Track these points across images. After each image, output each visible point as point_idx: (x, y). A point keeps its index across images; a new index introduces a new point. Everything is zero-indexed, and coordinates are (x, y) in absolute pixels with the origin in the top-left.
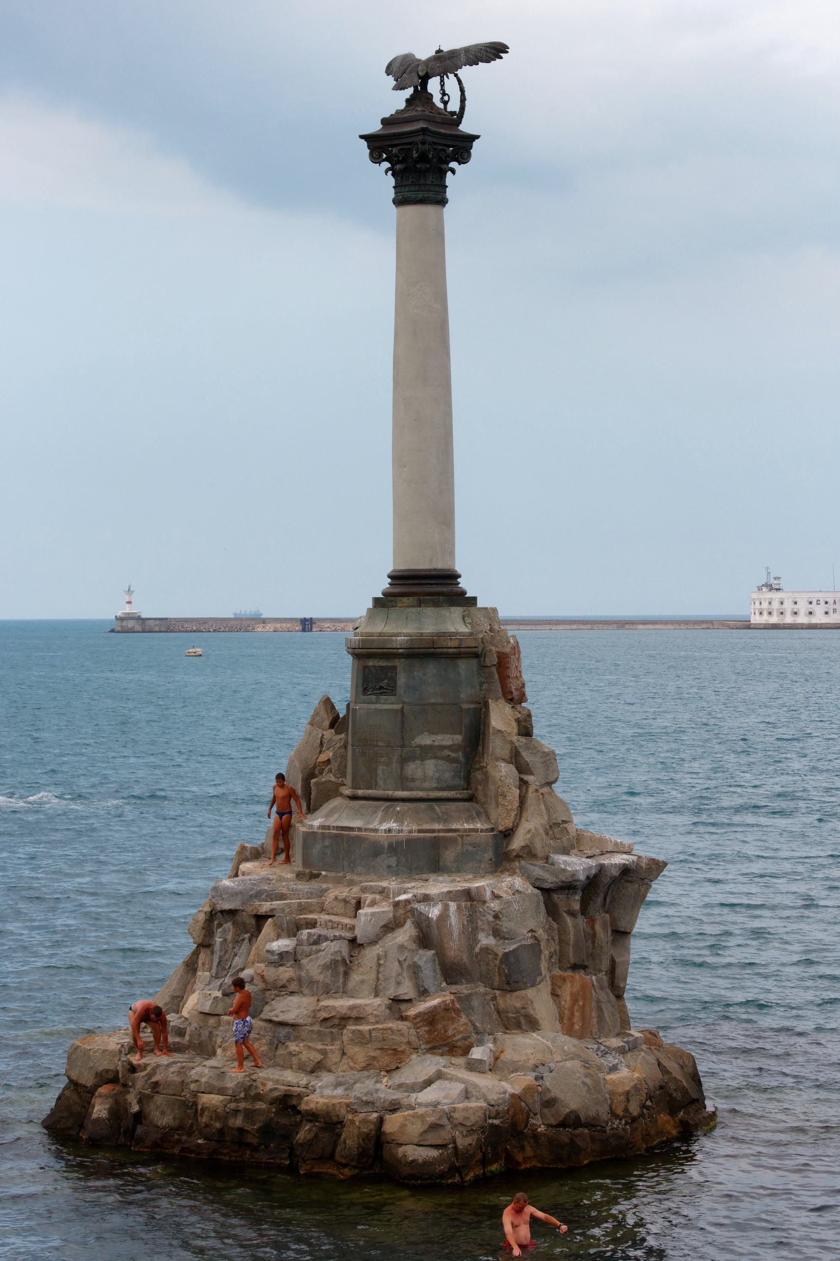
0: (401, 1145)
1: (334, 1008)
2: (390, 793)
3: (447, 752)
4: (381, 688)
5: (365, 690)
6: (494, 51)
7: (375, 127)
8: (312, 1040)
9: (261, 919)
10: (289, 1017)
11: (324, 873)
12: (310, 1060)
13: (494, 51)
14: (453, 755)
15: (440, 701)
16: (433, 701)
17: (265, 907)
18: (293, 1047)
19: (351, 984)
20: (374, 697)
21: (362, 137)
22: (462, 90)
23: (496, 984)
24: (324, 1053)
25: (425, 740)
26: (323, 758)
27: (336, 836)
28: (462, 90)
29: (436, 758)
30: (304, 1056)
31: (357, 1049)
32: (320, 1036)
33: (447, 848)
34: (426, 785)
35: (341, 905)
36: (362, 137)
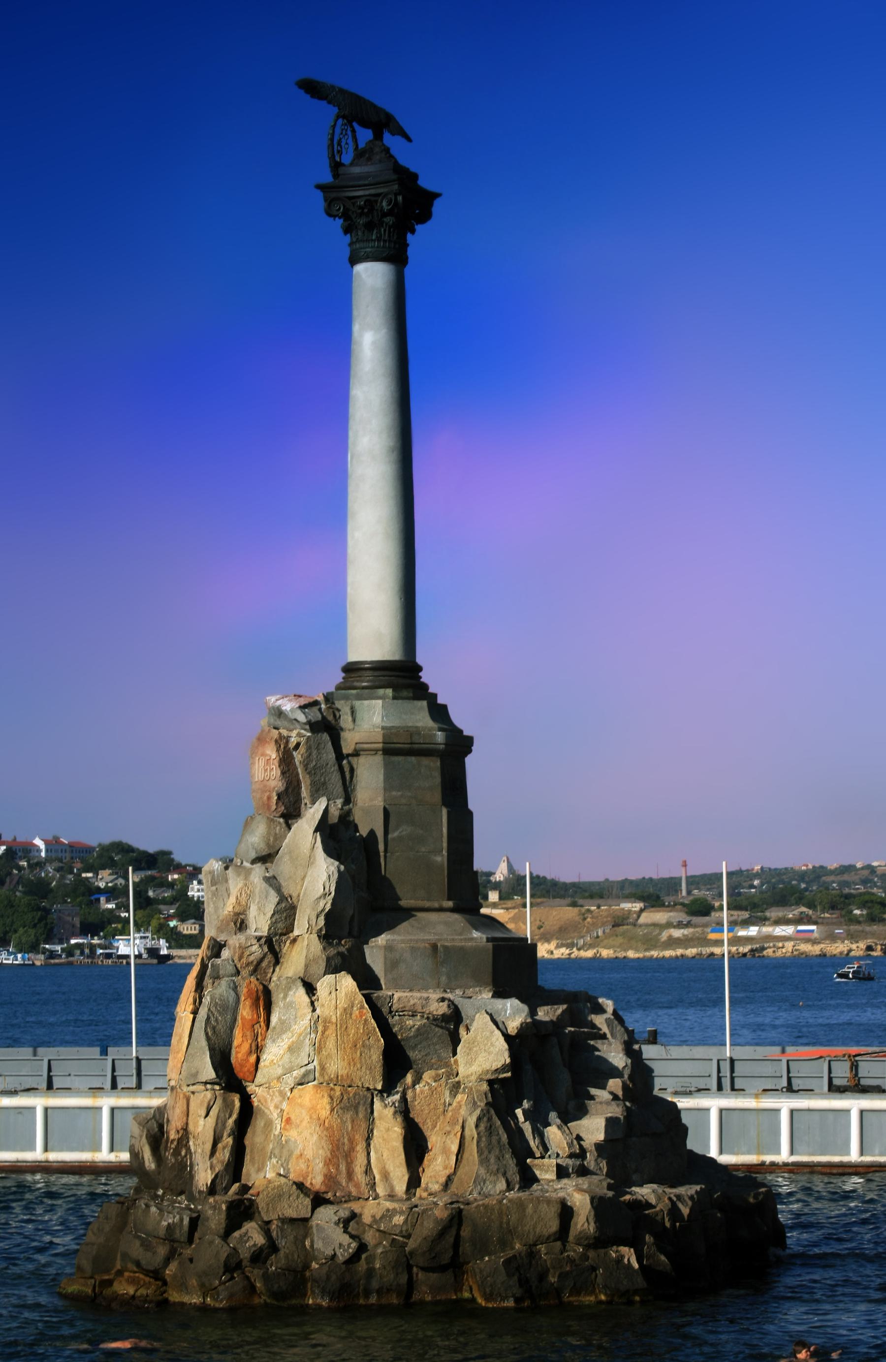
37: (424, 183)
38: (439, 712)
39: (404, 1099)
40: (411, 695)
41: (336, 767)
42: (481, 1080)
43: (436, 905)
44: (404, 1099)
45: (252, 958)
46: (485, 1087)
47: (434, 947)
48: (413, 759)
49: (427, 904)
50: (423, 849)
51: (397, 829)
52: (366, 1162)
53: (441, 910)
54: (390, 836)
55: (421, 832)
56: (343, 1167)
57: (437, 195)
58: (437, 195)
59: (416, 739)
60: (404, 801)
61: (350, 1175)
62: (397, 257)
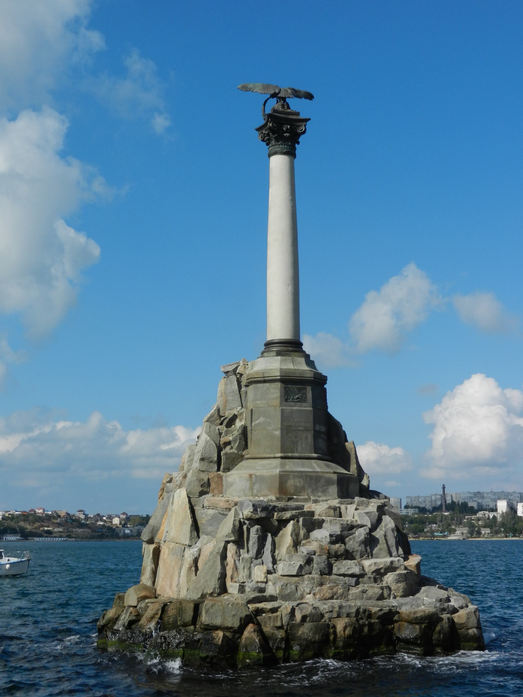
0: (469, 629)
1: (381, 563)
2: (310, 455)
5: (286, 400)
6: (309, 96)
8: (371, 583)
9: (283, 523)
10: (356, 570)
11: (295, 497)
12: (376, 593)
13: (309, 96)
17: (288, 515)
18: (360, 587)
19: (374, 552)
20: (293, 403)
24: (382, 588)
25: (318, 427)
26: (223, 440)
30: (370, 592)
31: (399, 585)
32: (375, 581)
35: (332, 511)
37: (302, 116)
38: (310, 363)
39: (200, 550)
40: (275, 354)
41: (238, 392)
42: (222, 541)
43: (272, 456)
44: (200, 550)
45: (177, 483)
46: (223, 544)
47: (251, 476)
48: (267, 385)
49: (268, 456)
50: (270, 428)
51: (258, 419)
52: (177, 581)
53: (275, 458)
54: (253, 424)
55: (269, 420)
56: (168, 583)
57: (309, 119)
58: (309, 119)
59: (266, 375)
60: (262, 406)
61: (171, 586)
62: (291, 153)
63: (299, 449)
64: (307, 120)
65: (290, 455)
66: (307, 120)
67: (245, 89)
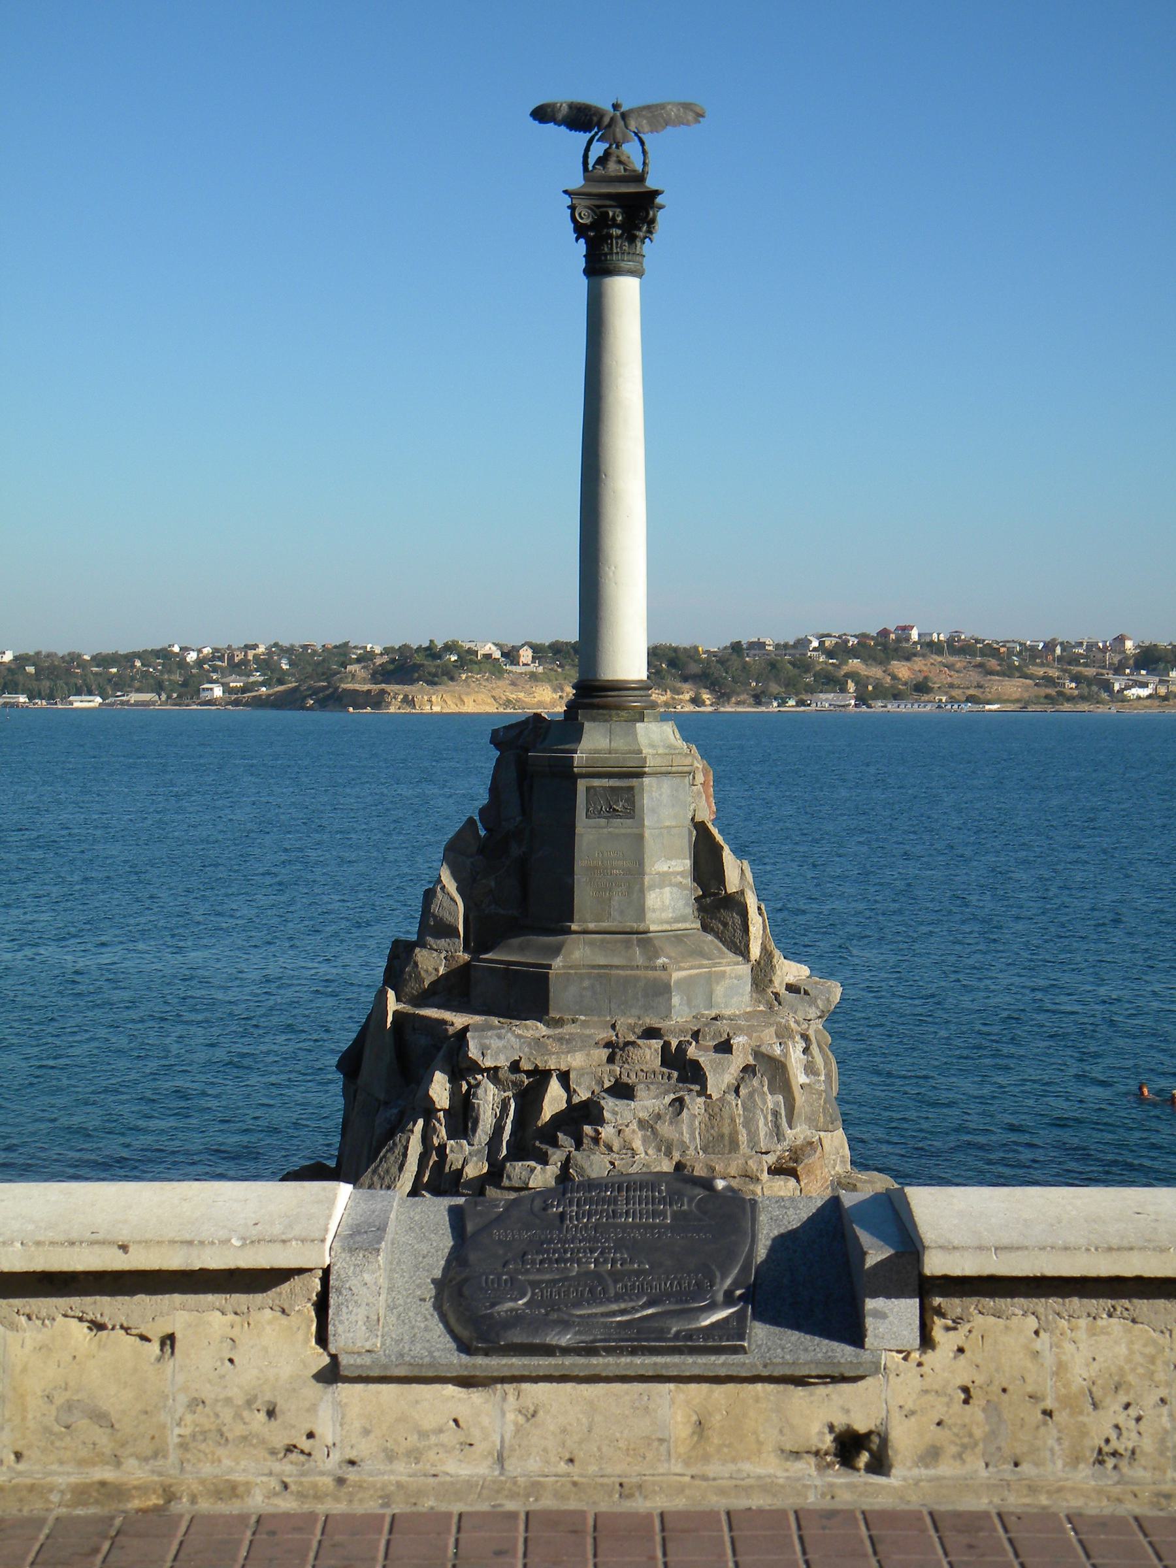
3: (679, 879)
4: (614, 810)
7: (577, 181)
11: (582, 1018)
14: (684, 881)
15: (674, 824)
16: (667, 824)
21: (566, 192)
22: (644, 152)
23: (820, 1125)
27: (600, 976)
28: (644, 152)
29: (671, 885)
33: (718, 983)
34: (664, 916)
36: (566, 192)
63: (615, 914)
64: (656, 193)
65: (592, 926)
66: (656, 193)
67: (542, 114)
